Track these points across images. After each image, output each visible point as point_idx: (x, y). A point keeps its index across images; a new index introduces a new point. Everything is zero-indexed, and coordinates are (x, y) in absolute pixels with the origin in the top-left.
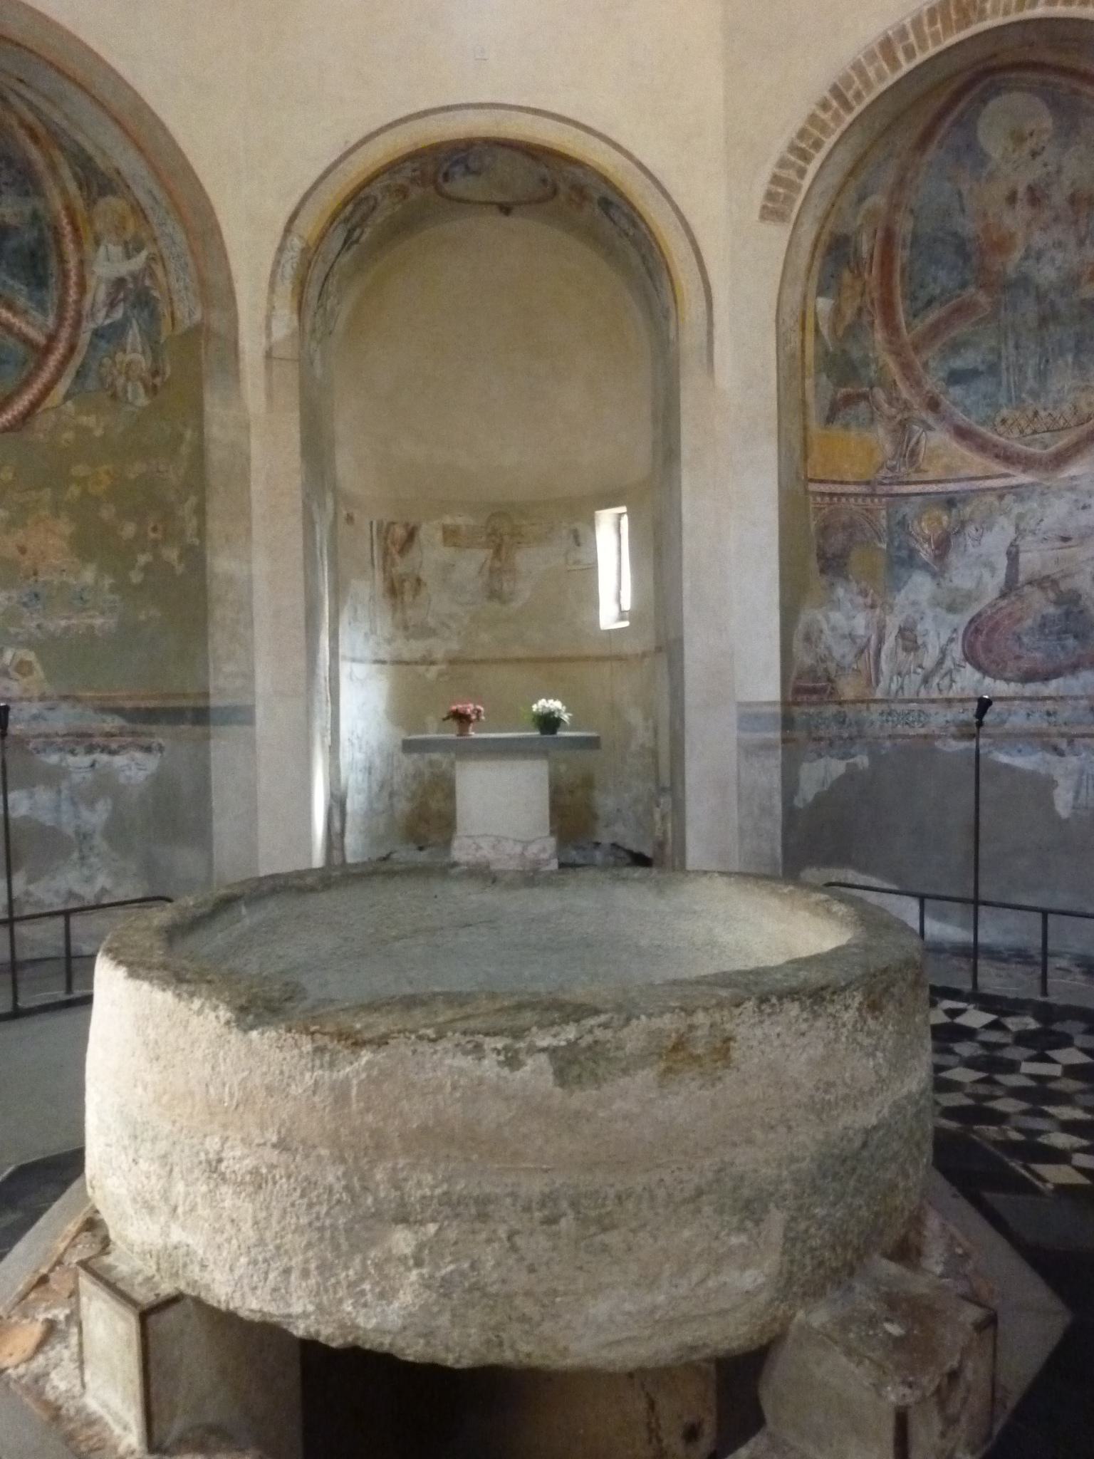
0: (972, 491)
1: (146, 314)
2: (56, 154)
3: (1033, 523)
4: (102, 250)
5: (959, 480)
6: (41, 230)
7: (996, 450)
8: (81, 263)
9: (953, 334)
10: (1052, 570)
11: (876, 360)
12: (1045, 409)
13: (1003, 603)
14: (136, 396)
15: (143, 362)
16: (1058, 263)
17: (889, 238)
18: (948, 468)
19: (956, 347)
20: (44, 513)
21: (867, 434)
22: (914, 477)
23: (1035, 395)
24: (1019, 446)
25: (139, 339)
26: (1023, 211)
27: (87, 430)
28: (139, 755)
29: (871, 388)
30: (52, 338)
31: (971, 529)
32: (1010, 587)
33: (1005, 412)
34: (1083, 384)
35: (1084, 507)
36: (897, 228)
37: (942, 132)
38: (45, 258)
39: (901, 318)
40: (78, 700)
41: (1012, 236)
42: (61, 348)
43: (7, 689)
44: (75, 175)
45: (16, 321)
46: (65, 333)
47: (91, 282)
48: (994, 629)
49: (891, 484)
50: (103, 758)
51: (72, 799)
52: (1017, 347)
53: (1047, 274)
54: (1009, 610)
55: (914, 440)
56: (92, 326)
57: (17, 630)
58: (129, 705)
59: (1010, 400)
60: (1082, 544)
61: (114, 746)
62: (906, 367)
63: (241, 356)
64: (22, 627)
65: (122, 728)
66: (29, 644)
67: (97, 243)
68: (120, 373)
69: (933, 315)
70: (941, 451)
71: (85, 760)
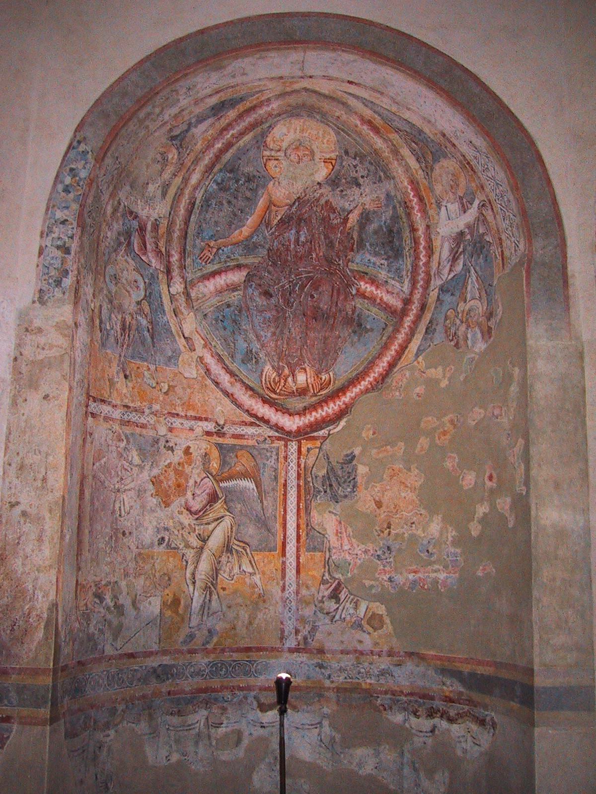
1: (481, 260)
2: (394, 136)
4: (443, 209)
6: (394, 207)
8: (428, 227)
14: (474, 343)
15: (479, 307)
20: (399, 466)
25: (477, 286)
27: (437, 381)
28: (474, 727)
30: (407, 302)
38: (399, 232)
40: (422, 658)
42: (414, 308)
43: (361, 642)
44: (413, 151)
45: (380, 293)
46: (417, 296)
47: (437, 243)
50: (444, 724)
51: (413, 763)
56: (439, 282)
57: (372, 583)
58: (466, 669)
61: (452, 713)
63: (571, 281)
64: (377, 579)
65: (461, 693)
66: (380, 598)
67: (439, 206)
68: (462, 322)
71: (426, 724)
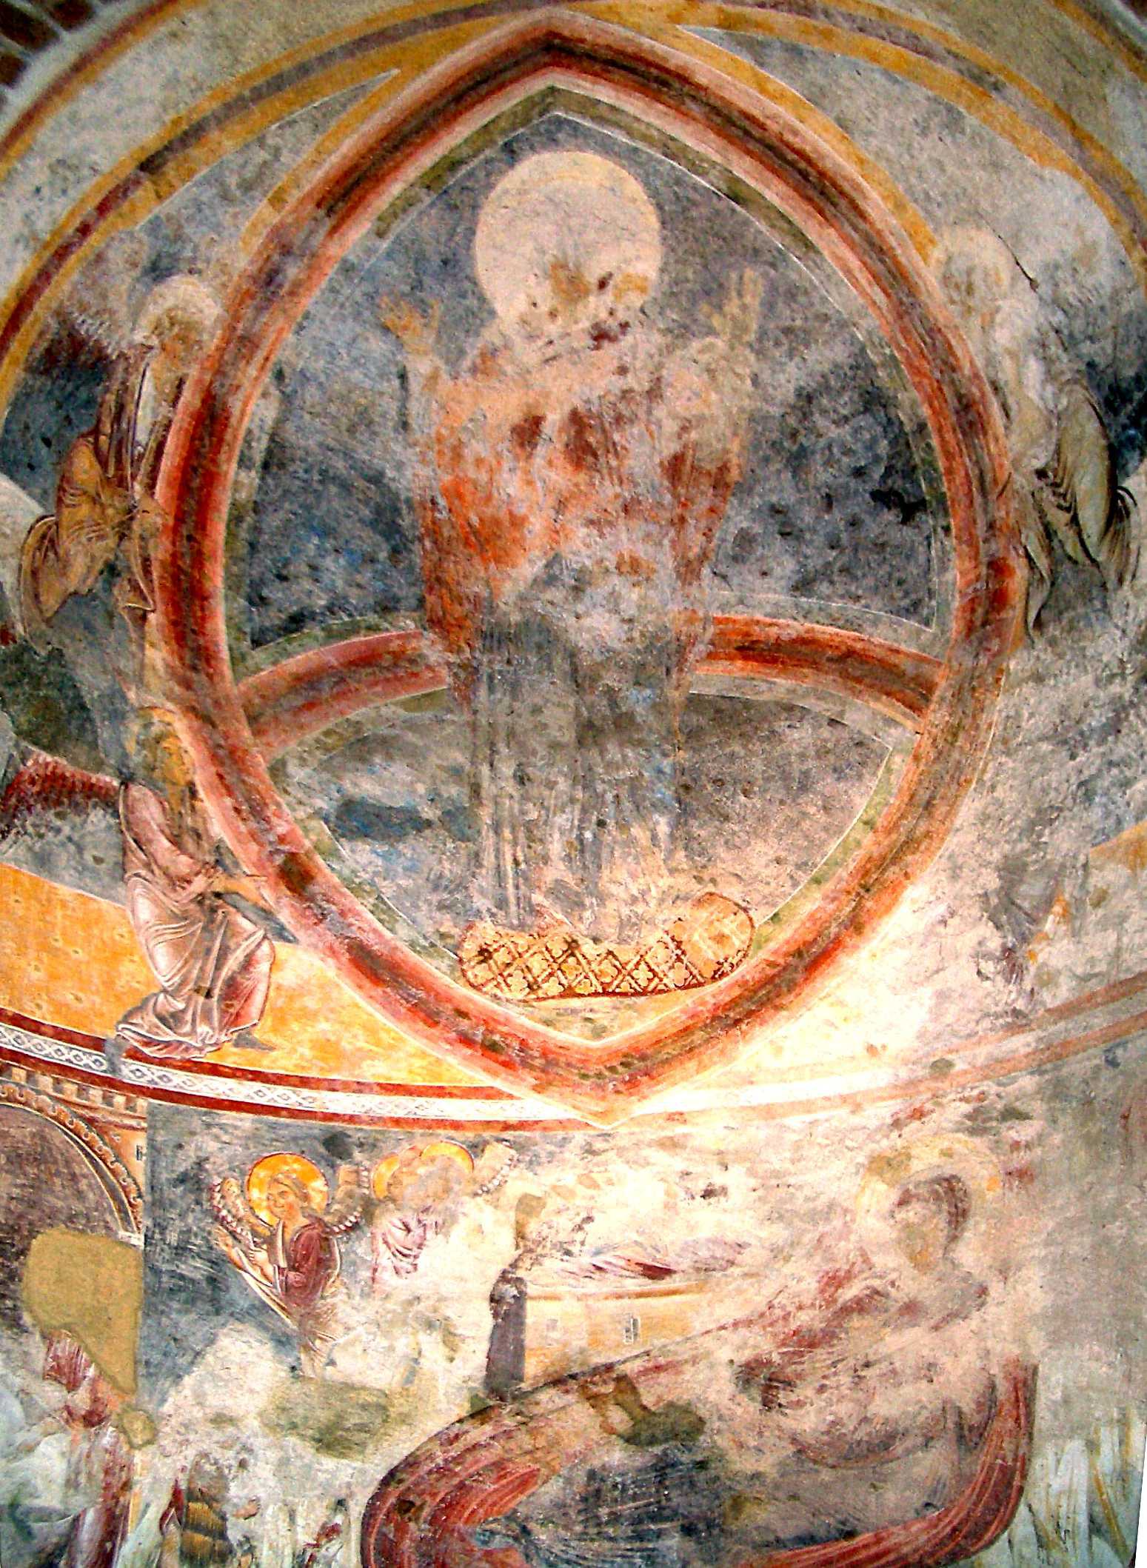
0: (397, 1122)
3: (564, 1224)
5: (360, 1087)
7: (464, 1024)
9: (353, 716)
10: (622, 1353)
11: (144, 712)
12: (596, 940)
13: (480, 1433)
16: (629, 610)
17: (211, 421)
18: (326, 1048)
19: (362, 747)
21: (105, 903)
22: (232, 1058)
23: (574, 904)
24: (522, 1019)
26: (550, 467)
29: (126, 782)
31: (388, 1223)
32: (500, 1389)
33: (486, 931)
34: (698, 890)
35: (708, 1194)
36: (235, 405)
37: (395, 189)
39: (220, 631)
41: (517, 522)
48: (450, 1506)
49: (162, 1062)
52: (522, 779)
53: (596, 626)
54: (498, 1449)
55: (232, 964)
59: (502, 903)
60: (700, 1289)
62: (228, 761)
69: (307, 654)
70: (311, 1003)
